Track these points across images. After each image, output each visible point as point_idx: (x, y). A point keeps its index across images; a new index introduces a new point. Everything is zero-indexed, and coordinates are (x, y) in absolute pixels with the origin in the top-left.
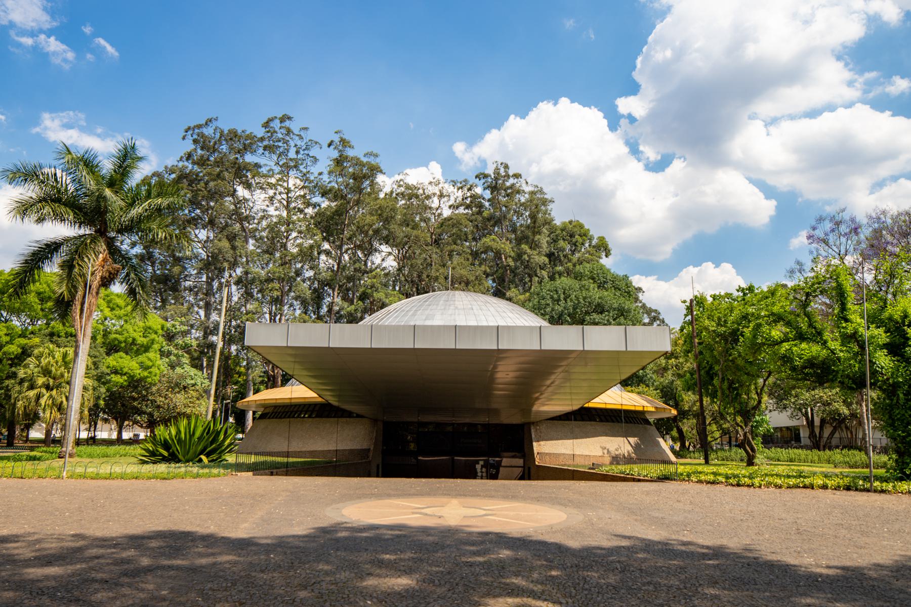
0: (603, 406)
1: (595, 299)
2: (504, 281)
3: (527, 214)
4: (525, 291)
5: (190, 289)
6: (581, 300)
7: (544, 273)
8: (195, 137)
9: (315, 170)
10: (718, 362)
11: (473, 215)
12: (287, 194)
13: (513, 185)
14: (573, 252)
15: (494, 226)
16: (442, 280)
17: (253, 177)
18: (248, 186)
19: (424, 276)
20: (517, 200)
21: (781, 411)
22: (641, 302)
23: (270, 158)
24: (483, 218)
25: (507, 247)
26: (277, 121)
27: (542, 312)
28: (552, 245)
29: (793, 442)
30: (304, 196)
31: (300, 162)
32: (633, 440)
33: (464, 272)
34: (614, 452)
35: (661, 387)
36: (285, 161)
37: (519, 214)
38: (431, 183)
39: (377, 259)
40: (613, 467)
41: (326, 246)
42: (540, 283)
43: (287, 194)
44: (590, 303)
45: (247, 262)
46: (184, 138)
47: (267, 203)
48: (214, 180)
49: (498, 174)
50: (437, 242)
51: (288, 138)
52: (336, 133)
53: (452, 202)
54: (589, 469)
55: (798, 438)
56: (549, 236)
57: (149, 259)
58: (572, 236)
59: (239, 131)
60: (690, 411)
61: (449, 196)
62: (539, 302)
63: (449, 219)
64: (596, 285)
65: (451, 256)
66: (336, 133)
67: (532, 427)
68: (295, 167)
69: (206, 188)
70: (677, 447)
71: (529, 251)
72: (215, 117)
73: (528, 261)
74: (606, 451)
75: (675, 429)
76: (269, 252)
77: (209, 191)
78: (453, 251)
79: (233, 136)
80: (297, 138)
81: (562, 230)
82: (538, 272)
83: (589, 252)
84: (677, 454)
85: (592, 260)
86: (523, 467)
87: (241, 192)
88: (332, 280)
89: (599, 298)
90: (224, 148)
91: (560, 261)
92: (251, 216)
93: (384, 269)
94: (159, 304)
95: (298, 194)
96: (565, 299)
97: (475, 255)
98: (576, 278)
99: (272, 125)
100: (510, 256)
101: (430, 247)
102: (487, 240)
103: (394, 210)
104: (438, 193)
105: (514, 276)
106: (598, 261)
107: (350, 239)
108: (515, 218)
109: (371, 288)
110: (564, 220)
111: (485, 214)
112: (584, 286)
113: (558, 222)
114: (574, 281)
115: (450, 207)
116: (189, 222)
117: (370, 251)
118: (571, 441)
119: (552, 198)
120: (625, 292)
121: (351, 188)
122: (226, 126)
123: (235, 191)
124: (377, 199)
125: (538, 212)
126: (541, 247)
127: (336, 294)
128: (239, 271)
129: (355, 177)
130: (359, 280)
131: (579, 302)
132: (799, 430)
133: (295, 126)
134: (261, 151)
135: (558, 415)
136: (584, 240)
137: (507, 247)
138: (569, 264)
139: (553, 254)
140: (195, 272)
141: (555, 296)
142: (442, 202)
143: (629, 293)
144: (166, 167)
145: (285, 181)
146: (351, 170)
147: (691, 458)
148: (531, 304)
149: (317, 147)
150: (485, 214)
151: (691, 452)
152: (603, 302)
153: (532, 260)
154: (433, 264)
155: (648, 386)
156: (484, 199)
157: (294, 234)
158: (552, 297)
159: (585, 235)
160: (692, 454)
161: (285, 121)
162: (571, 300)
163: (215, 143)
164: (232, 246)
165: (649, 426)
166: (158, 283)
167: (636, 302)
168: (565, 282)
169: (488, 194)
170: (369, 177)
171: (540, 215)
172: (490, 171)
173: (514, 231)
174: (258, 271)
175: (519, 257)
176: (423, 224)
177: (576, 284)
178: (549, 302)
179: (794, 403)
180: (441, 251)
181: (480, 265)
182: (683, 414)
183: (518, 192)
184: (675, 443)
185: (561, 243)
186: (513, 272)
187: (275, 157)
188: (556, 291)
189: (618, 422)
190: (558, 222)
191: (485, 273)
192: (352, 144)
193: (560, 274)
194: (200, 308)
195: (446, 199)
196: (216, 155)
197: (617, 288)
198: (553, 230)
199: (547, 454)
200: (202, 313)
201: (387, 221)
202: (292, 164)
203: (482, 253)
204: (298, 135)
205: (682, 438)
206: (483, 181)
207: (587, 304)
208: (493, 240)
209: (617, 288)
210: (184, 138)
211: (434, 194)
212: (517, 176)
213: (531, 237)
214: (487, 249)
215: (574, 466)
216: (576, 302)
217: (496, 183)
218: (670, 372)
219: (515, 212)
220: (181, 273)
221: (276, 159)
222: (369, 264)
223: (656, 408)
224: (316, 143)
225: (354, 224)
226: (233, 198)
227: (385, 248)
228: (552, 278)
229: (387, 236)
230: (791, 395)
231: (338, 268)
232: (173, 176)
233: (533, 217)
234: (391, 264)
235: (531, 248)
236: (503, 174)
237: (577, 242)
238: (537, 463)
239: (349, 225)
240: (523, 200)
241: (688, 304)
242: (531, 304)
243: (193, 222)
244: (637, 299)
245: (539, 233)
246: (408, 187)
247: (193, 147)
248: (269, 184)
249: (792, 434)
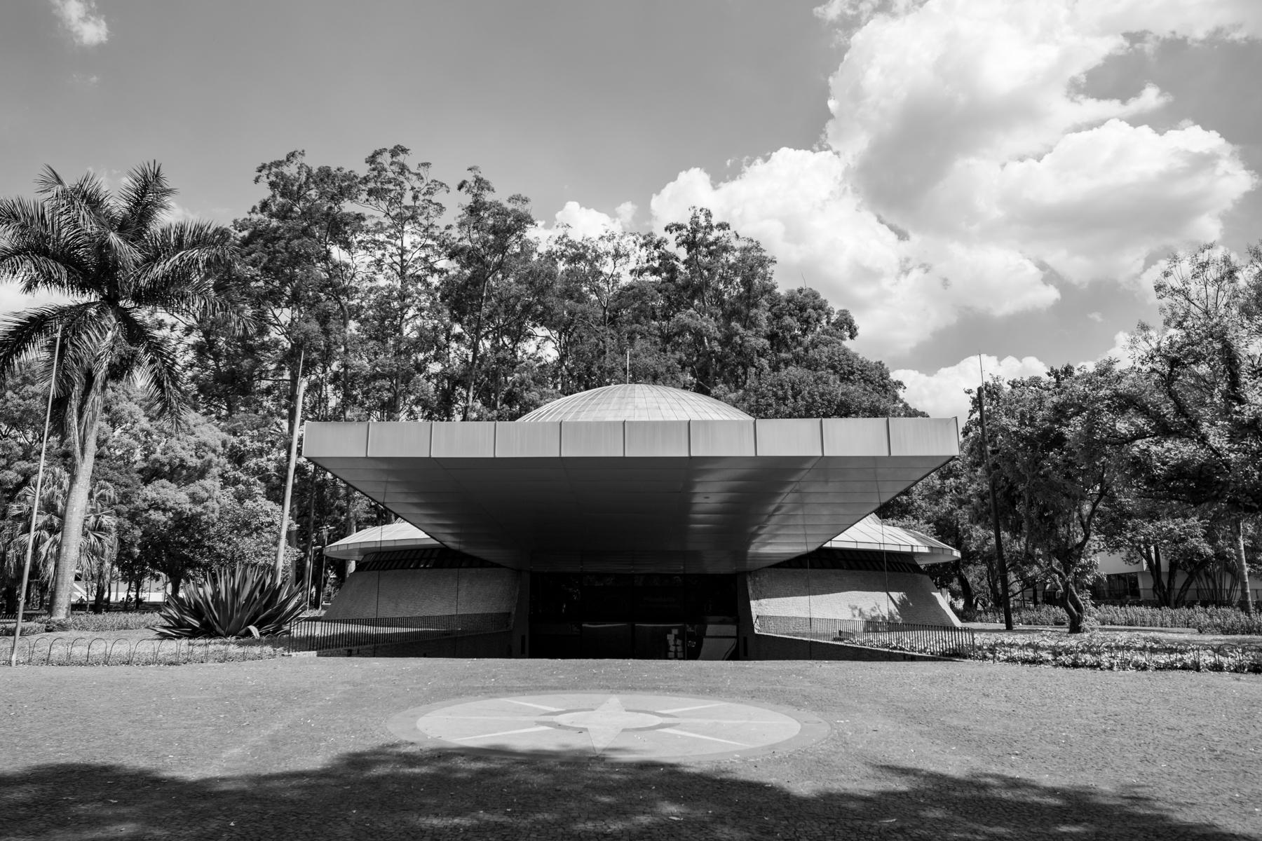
0: (853, 546)
1: (836, 396)
2: (707, 374)
3: (738, 280)
4: (738, 388)
5: (268, 391)
6: (817, 398)
7: (764, 362)
8: (273, 178)
9: (441, 222)
11: (663, 282)
12: (401, 255)
13: (718, 239)
14: (804, 332)
15: (692, 298)
16: (620, 374)
17: (354, 232)
18: (347, 245)
19: (595, 369)
20: (723, 261)
21: (1112, 552)
22: (901, 401)
23: (378, 206)
24: (677, 286)
25: (710, 325)
26: (387, 155)
28: (774, 323)
29: (1128, 597)
30: (426, 260)
31: (419, 211)
33: (649, 361)
34: (869, 614)
35: (935, 519)
36: (399, 210)
37: (727, 281)
38: (602, 238)
39: (529, 347)
40: (871, 637)
41: (457, 329)
42: (758, 375)
43: (401, 255)
44: (829, 401)
45: (346, 351)
46: (257, 181)
47: (373, 268)
48: (299, 238)
49: (697, 223)
50: (613, 321)
51: (401, 178)
52: (470, 169)
53: (632, 265)
54: (835, 639)
55: (1135, 592)
56: (769, 310)
57: (210, 349)
58: (802, 309)
59: (333, 169)
60: (977, 553)
61: (628, 255)
62: (757, 402)
63: (631, 287)
64: (837, 376)
65: (631, 339)
66: (470, 169)
67: (749, 578)
68: (413, 217)
69: (286, 249)
70: (960, 604)
71: (741, 330)
72: (300, 150)
73: (740, 346)
74: (857, 612)
75: (956, 579)
76: (380, 336)
77: (291, 253)
78: (634, 332)
79: (325, 175)
80: (415, 178)
81: (789, 301)
83: (825, 332)
84: (961, 615)
85: (831, 342)
86: (737, 637)
87: (337, 253)
88: (466, 375)
89: (842, 394)
90: (313, 193)
91: (787, 345)
92: (351, 287)
93: (540, 359)
94: (224, 412)
95: (416, 256)
96: (794, 397)
97: (667, 338)
98: (808, 367)
99: (379, 160)
100: (716, 339)
101: (602, 328)
102: (683, 317)
103: (551, 276)
104: (613, 252)
105: (722, 368)
106: (839, 344)
107: (489, 317)
108: (721, 286)
109: (521, 385)
110: (790, 288)
111: (680, 280)
112: (820, 378)
113: (782, 290)
114: (806, 370)
115: (632, 272)
116: (265, 297)
117: (519, 335)
118: (807, 597)
119: (774, 257)
120: (880, 386)
121: (490, 247)
122: (315, 163)
123: (328, 252)
124: (526, 261)
125: (753, 276)
126: (761, 326)
127: (471, 394)
128: (335, 366)
129: (494, 230)
130: (505, 375)
131: (815, 401)
132: (1136, 579)
133: (411, 161)
134: (364, 196)
135: (785, 559)
136: (820, 315)
137: (710, 325)
138: (799, 349)
139: (776, 335)
140: (274, 366)
141: (780, 393)
142: (618, 265)
143: (884, 386)
144: (235, 221)
145: (398, 238)
146: (491, 222)
147: (981, 621)
148: (746, 405)
149: (443, 190)
150: (680, 280)
151: (980, 612)
152: (849, 400)
153: (746, 344)
154: (607, 350)
155: (915, 517)
156: (677, 259)
157: (411, 312)
158: (775, 394)
159: (821, 307)
160: (983, 615)
161: (398, 154)
162: (803, 399)
163: (300, 187)
164: (324, 329)
165: (919, 576)
166: (223, 382)
167: (894, 402)
168: (794, 372)
169: (683, 253)
170: (516, 230)
171: (756, 281)
172: (686, 221)
173: (721, 303)
174: (362, 363)
175: (727, 341)
176: (594, 297)
177: (809, 376)
178: (772, 401)
179: (1130, 539)
180: (618, 333)
181: (673, 352)
182: (968, 557)
183: (725, 249)
184: (956, 600)
185: (788, 320)
186: (721, 361)
187: (384, 205)
188: (781, 385)
189: (875, 569)
190: (782, 290)
191: (680, 361)
192: (493, 185)
193: (787, 363)
194: (283, 418)
195: (623, 260)
196: (301, 203)
197: (867, 380)
198: (775, 301)
199: (771, 617)
200: (285, 424)
201: (541, 291)
202: (408, 214)
203: (676, 334)
204: (416, 174)
205: (966, 592)
206: (675, 234)
207: (826, 403)
208: (691, 316)
209: (867, 380)
210: (257, 181)
211: (607, 253)
212: (723, 226)
213: (745, 312)
214: (683, 329)
215: (812, 635)
216: (810, 400)
217: (695, 237)
218: (948, 497)
219: (722, 277)
220: (253, 368)
221: (385, 208)
222: (520, 353)
223: (931, 548)
224: (442, 185)
225: (495, 296)
226: (326, 264)
227: (541, 332)
228: (775, 368)
229: (542, 314)
230: (1126, 527)
231: (474, 357)
232: (246, 233)
233: (747, 283)
234: (550, 353)
235: (744, 327)
236: (704, 224)
237: (809, 317)
238: (756, 632)
239: (488, 298)
240: (732, 260)
242: (746, 405)
243: (274, 297)
244: (896, 397)
245: (756, 305)
246: (571, 244)
247: (270, 193)
248: (375, 242)
249: (1125, 586)
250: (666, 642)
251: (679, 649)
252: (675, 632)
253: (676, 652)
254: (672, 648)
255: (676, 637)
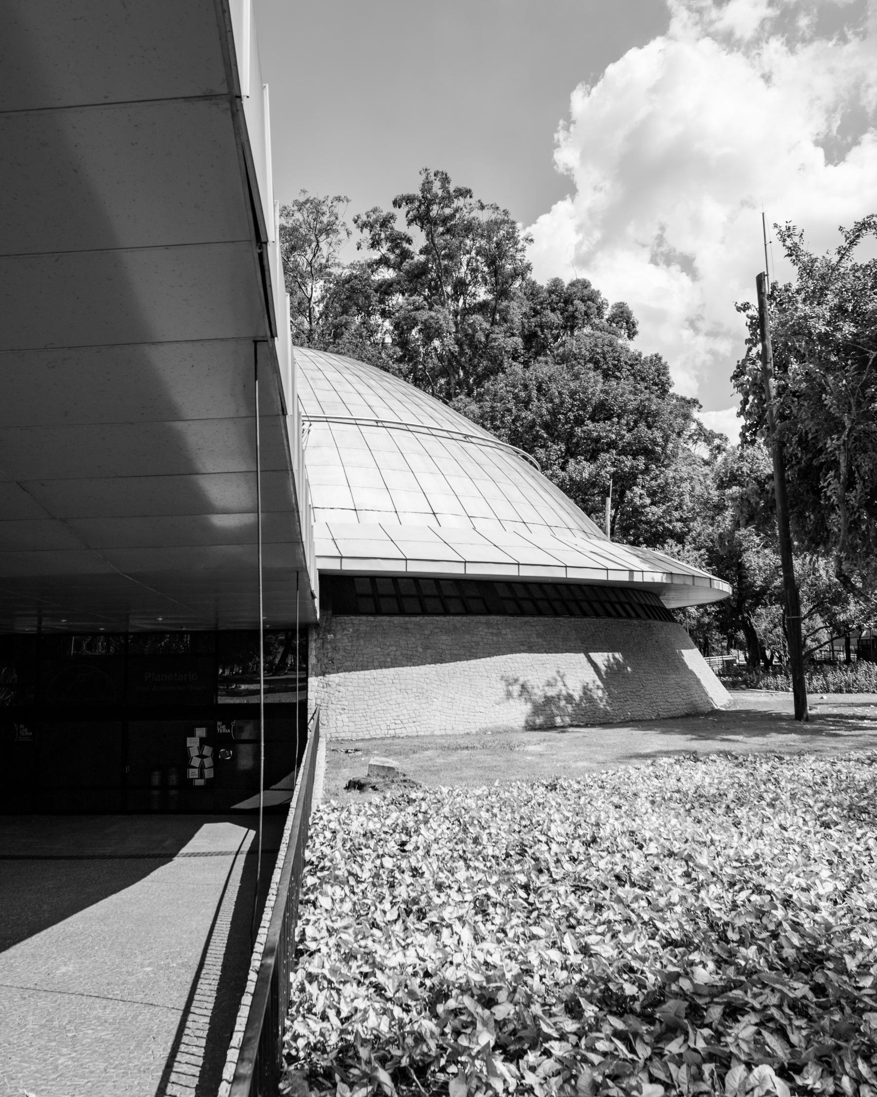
1: (593, 394)
6: (568, 399)
10: (836, 426)
27: (498, 423)
32: (600, 658)
81: (551, 292)
82: (506, 365)
89: (602, 391)
120: (655, 384)
141: (523, 394)
158: (516, 397)
162: (551, 401)
177: (562, 372)
178: (511, 405)
241: (754, 312)
250: (186, 751)
251: (208, 762)
252: (201, 732)
253: (202, 767)
254: (196, 762)
255: (203, 742)
